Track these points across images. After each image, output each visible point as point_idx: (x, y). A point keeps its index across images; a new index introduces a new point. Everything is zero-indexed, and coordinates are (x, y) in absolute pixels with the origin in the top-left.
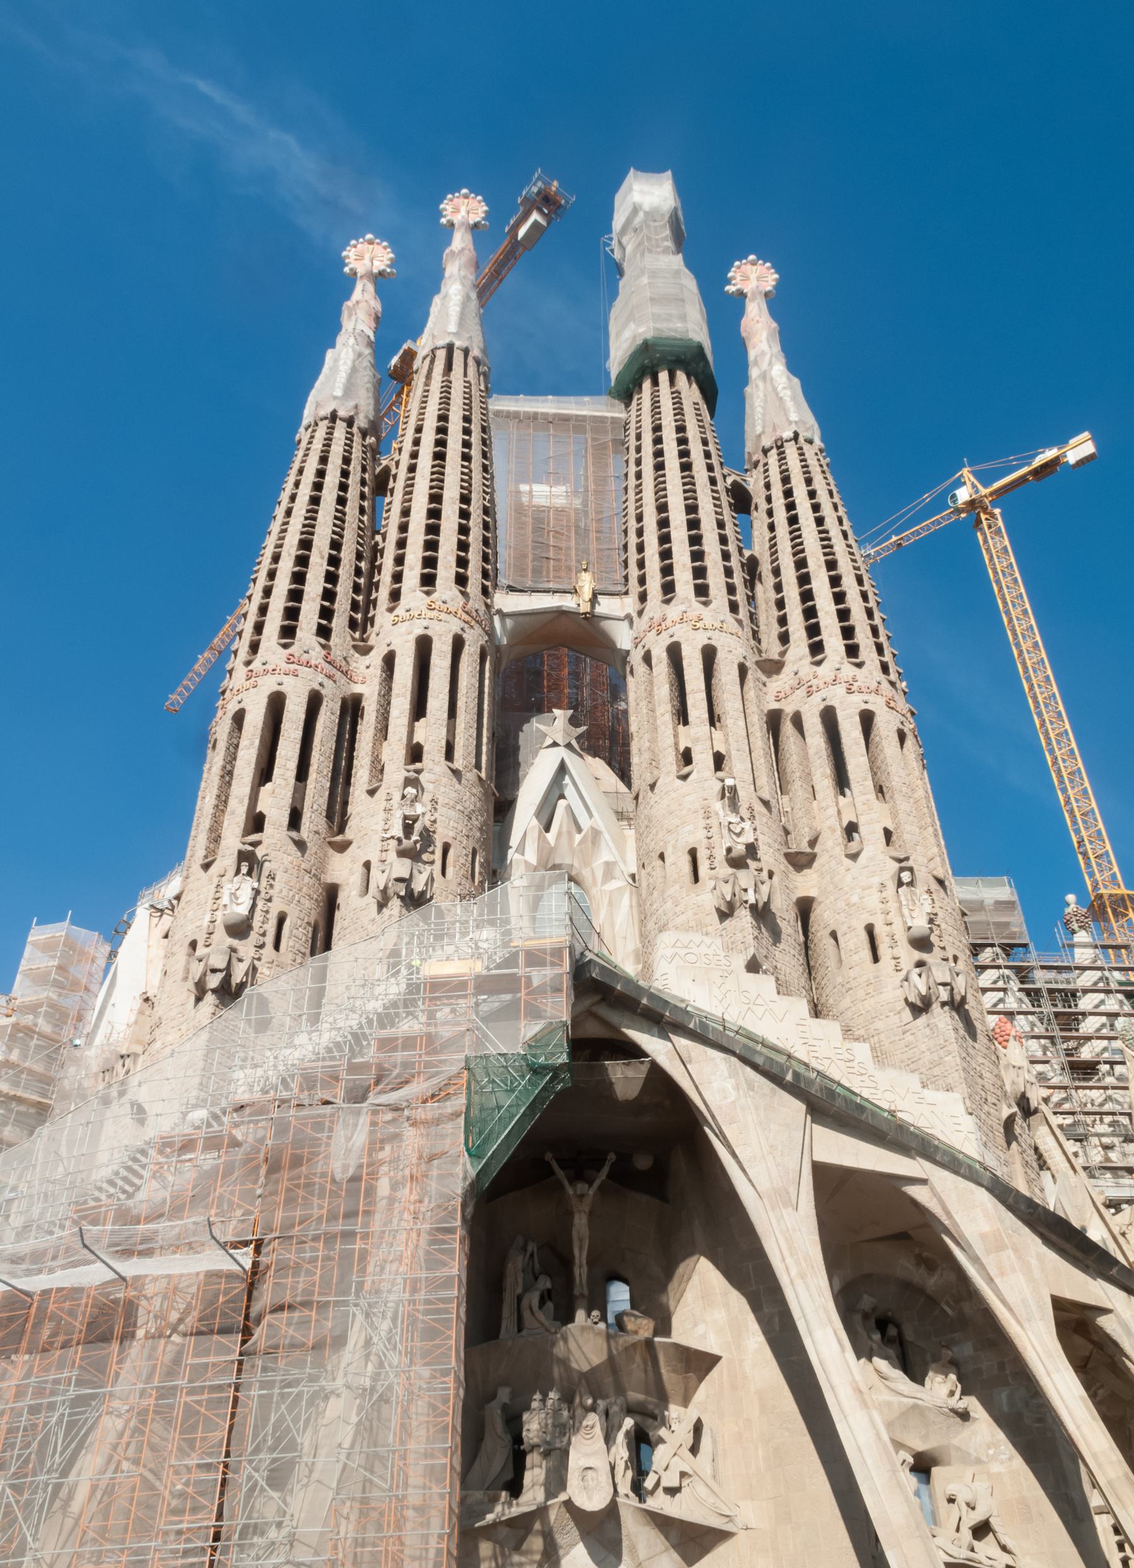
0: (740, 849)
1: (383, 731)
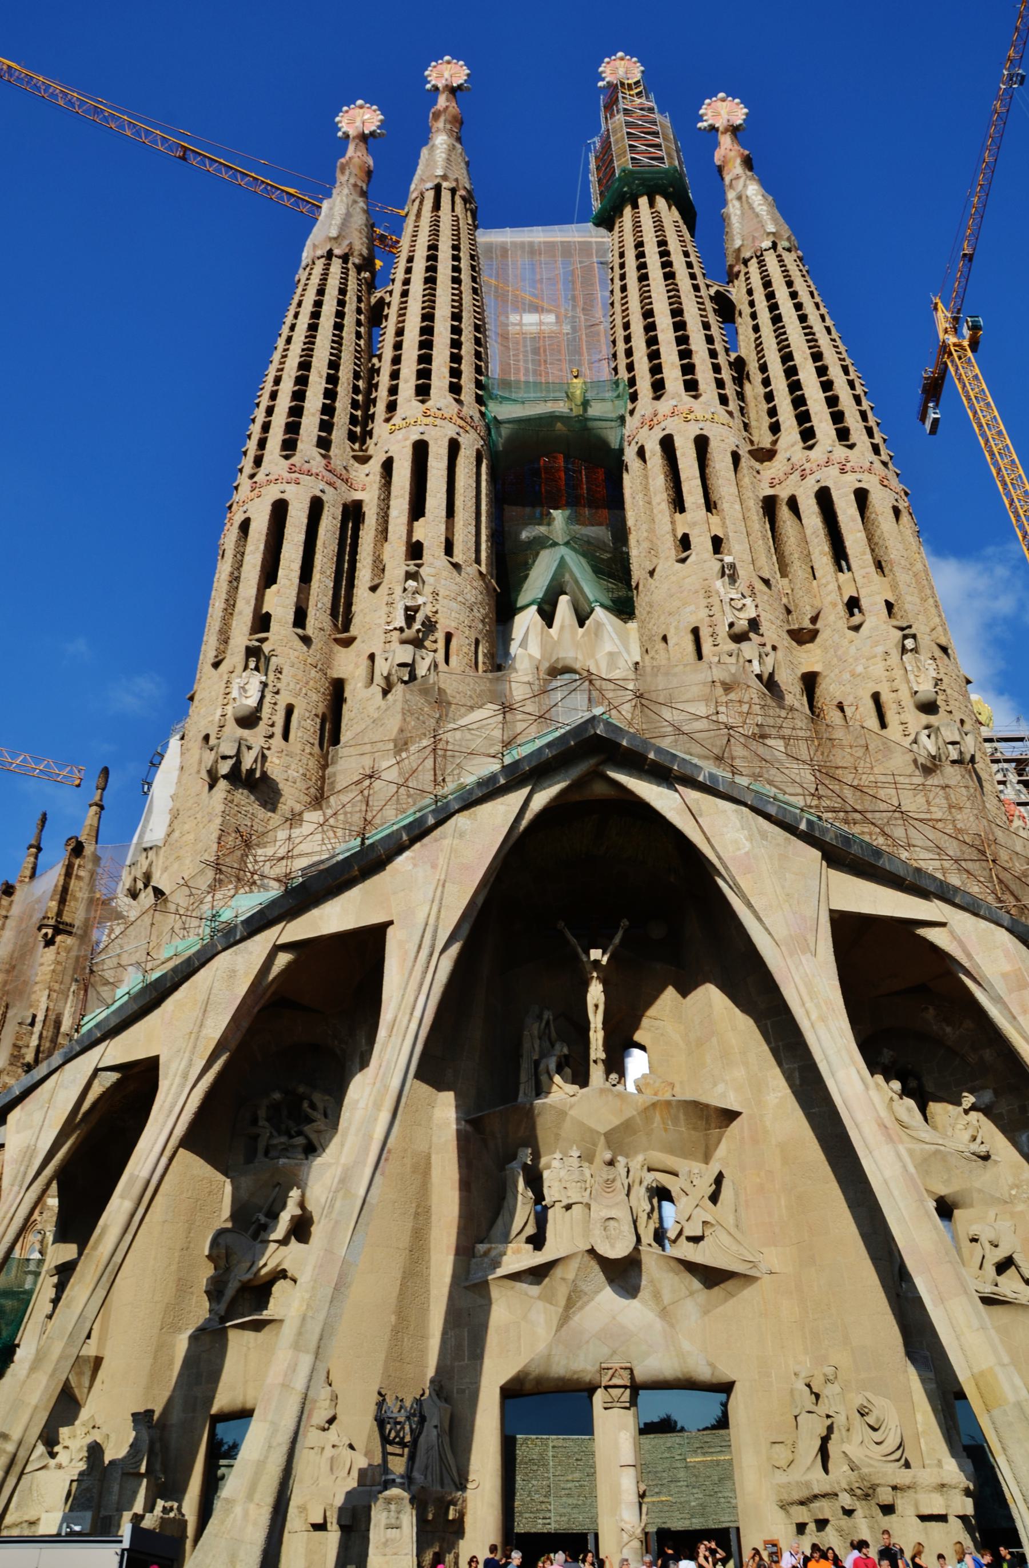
0: (742, 624)
1: (383, 532)
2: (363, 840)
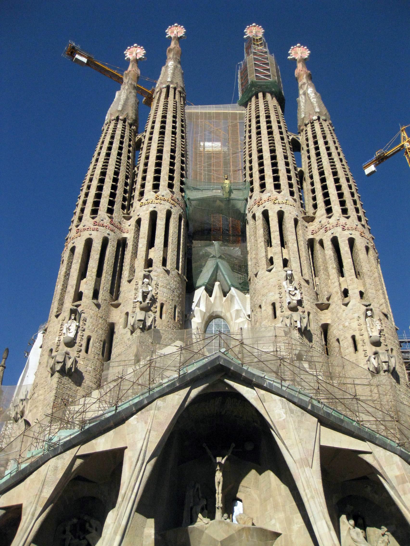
2: (116, 407)
